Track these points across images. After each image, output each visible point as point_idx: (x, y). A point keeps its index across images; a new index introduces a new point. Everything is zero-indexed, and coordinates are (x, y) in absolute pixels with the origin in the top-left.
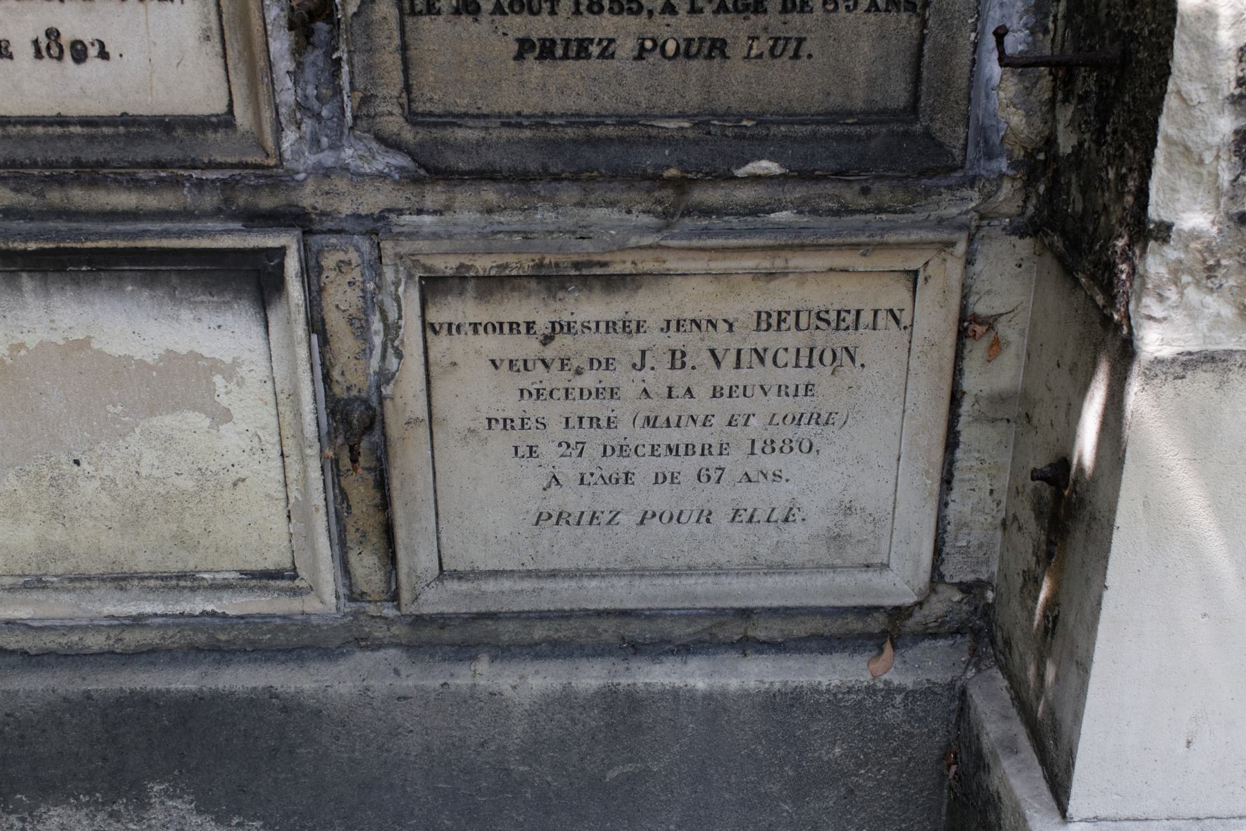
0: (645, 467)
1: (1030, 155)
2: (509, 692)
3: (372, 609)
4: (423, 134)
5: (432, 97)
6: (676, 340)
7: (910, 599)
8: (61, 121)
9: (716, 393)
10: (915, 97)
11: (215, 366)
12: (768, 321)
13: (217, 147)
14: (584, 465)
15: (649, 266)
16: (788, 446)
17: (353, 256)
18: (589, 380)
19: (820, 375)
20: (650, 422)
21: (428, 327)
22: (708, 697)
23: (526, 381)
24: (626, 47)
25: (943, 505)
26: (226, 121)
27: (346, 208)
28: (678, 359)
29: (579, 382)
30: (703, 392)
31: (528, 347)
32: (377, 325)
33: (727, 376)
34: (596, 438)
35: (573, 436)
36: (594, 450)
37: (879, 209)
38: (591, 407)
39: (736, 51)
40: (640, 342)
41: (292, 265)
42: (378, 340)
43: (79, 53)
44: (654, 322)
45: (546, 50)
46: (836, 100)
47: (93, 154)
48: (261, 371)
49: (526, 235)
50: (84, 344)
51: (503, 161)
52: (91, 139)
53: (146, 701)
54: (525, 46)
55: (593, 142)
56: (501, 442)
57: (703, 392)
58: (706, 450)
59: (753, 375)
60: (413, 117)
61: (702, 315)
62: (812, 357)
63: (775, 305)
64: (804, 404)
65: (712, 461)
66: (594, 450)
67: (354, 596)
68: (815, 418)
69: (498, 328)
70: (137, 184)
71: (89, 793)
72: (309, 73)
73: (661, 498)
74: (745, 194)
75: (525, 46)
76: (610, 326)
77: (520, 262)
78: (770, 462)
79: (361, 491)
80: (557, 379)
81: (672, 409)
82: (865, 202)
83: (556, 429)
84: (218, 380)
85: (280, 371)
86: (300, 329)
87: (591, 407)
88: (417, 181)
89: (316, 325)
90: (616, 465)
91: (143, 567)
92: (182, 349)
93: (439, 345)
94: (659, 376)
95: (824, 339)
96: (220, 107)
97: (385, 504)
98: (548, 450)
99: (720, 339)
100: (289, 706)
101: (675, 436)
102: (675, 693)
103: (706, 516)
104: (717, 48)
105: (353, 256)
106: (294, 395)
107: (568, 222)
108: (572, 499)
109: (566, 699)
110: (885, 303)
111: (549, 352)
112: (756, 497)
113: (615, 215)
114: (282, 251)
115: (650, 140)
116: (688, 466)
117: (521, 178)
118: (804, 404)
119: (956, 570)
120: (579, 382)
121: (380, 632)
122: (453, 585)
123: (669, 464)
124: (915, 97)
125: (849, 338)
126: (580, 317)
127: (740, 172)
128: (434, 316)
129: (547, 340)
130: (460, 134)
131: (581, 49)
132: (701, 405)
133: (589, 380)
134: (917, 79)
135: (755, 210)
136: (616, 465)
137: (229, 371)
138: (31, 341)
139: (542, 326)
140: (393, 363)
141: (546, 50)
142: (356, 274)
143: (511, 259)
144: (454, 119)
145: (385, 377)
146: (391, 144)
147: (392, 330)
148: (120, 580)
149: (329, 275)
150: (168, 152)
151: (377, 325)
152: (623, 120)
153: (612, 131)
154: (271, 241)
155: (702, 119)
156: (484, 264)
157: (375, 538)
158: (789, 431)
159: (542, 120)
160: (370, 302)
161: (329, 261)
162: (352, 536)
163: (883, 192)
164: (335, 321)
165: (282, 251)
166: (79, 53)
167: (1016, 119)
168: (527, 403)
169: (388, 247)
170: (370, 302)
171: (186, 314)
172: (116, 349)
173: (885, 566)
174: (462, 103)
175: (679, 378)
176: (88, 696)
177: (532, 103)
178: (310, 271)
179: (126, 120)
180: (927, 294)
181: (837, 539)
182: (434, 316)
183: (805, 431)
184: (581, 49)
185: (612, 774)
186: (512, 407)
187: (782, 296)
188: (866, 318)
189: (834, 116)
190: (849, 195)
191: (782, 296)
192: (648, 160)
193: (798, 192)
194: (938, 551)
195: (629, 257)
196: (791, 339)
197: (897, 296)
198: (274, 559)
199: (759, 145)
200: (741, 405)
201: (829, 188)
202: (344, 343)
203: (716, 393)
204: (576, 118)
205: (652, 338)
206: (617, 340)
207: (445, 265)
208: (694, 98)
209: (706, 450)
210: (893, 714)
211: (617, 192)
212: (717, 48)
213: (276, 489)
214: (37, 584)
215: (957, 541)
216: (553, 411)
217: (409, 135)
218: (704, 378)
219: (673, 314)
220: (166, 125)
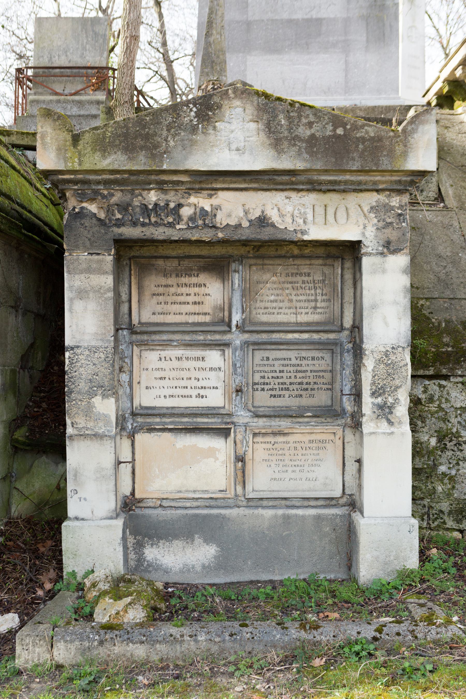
0: (290, 469)
1: (352, 414)
2: (265, 515)
3: (240, 498)
4: (255, 409)
5: (256, 404)
6: (295, 445)
7: (339, 496)
8: (198, 407)
9: (302, 455)
10: (332, 404)
11: (217, 449)
12: (311, 442)
13: (222, 411)
14: (279, 469)
15: (290, 432)
16: (315, 465)
17: (242, 430)
18: (280, 452)
19: (320, 452)
20: (291, 460)
21: (253, 442)
22: (303, 516)
23: (269, 452)
24: (287, 396)
25: (343, 477)
26: (224, 407)
27: (241, 422)
28: (295, 448)
29: (279, 453)
30: (300, 455)
31: (270, 446)
32: (245, 442)
33: (304, 452)
34: (281, 463)
35: (277, 463)
36: (281, 466)
37: (328, 422)
38: (281, 457)
39: (304, 396)
40: (289, 445)
41: (232, 430)
42: (245, 445)
43: (202, 397)
44: (292, 442)
45: (275, 396)
46: (320, 404)
47: (203, 412)
48: (225, 451)
49: (271, 426)
50: (196, 445)
51: (268, 414)
52: (202, 410)
53: (196, 516)
54: (271, 395)
55: (282, 410)
56: (265, 464)
57: (300, 455)
58: (301, 466)
59: (308, 452)
60: (253, 407)
61: (300, 441)
62: (319, 448)
63: (312, 439)
64: (318, 457)
65: (302, 468)
66: (281, 466)
67: (236, 495)
68: (320, 460)
69: (265, 443)
70: (208, 418)
71: (183, 537)
72: (237, 400)
73: (293, 475)
74: (306, 420)
75: (271, 395)
76: (284, 442)
77: (269, 431)
78: (313, 468)
79: (240, 474)
80: (275, 452)
81: (295, 458)
82: (326, 421)
83: (275, 461)
84: (217, 452)
85: (228, 450)
86: (233, 442)
87: (281, 457)
88: (253, 417)
89: (235, 442)
90: (285, 469)
91: (199, 489)
92: (212, 446)
93: (255, 445)
94: (292, 452)
95: (320, 445)
96: (223, 405)
97: (244, 476)
98: (273, 465)
99: (302, 445)
100: (224, 517)
101: (295, 463)
102: (296, 515)
103: (301, 479)
104: (301, 396)
105: (242, 430)
106: (230, 454)
107: (277, 424)
108: (277, 476)
109: (276, 516)
110: (330, 439)
111: (274, 447)
112: (310, 475)
113: (285, 423)
114: (231, 428)
115: (291, 410)
116: (298, 469)
117: (269, 416)
118: (318, 457)
119: (348, 492)
120: (279, 453)
121: (240, 503)
122: (254, 493)
123: (294, 468)
124: (332, 404)
125: (325, 445)
126: (279, 441)
127: (305, 415)
128: (255, 440)
129: (273, 445)
130: (261, 409)
131: (280, 396)
132: (300, 457)
133: (280, 452)
134: (332, 401)
135: (308, 422)
136: (285, 469)
137: (219, 450)
138: (187, 445)
139: (273, 443)
140: (247, 449)
141: (275, 396)
142: (242, 433)
143: (268, 430)
144: (259, 407)
145: (246, 451)
146: (250, 411)
147: (247, 442)
148: (195, 491)
149: (238, 433)
150: (215, 412)
151: (245, 442)
152: (286, 407)
153: (285, 409)
154: (230, 427)
155: (299, 407)
156: (263, 431)
157: (242, 484)
158: (315, 462)
159: (274, 407)
160: (244, 437)
161: (238, 431)
162: (237, 482)
163: (329, 420)
164: (238, 441)
165: (231, 428)
166: (202, 397)
167: (349, 408)
168: (270, 456)
169: (248, 428)
170: (244, 437)
171: (213, 440)
172: (200, 446)
173: (334, 490)
174: (261, 405)
175: (296, 452)
176: (187, 514)
177: (272, 404)
178: (235, 432)
179: (208, 407)
180: (337, 437)
181: (325, 484)
182: (254, 441)
183: (318, 462)
184: (280, 396)
185: (284, 534)
186: (267, 457)
187: (313, 437)
188: (327, 441)
189: (319, 407)
190: (323, 420)
191: (313, 437)
192: (290, 413)
193: (315, 419)
194: (344, 485)
195: (287, 430)
196: (314, 445)
197: (332, 437)
198: (223, 488)
199: (309, 411)
200: (306, 457)
201: (320, 419)
202: (239, 445)
203: (302, 455)
204: (278, 407)
205: (291, 445)
206: (285, 445)
207: (257, 431)
208: (297, 404)
209: (301, 466)
210: (338, 520)
211: (285, 419)
212: (301, 396)
213: (225, 473)
214: (180, 492)
215: (346, 484)
216: (274, 458)
217: (253, 409)
218: (300, 452)
219: (295, 440)
220: (214, 408)
